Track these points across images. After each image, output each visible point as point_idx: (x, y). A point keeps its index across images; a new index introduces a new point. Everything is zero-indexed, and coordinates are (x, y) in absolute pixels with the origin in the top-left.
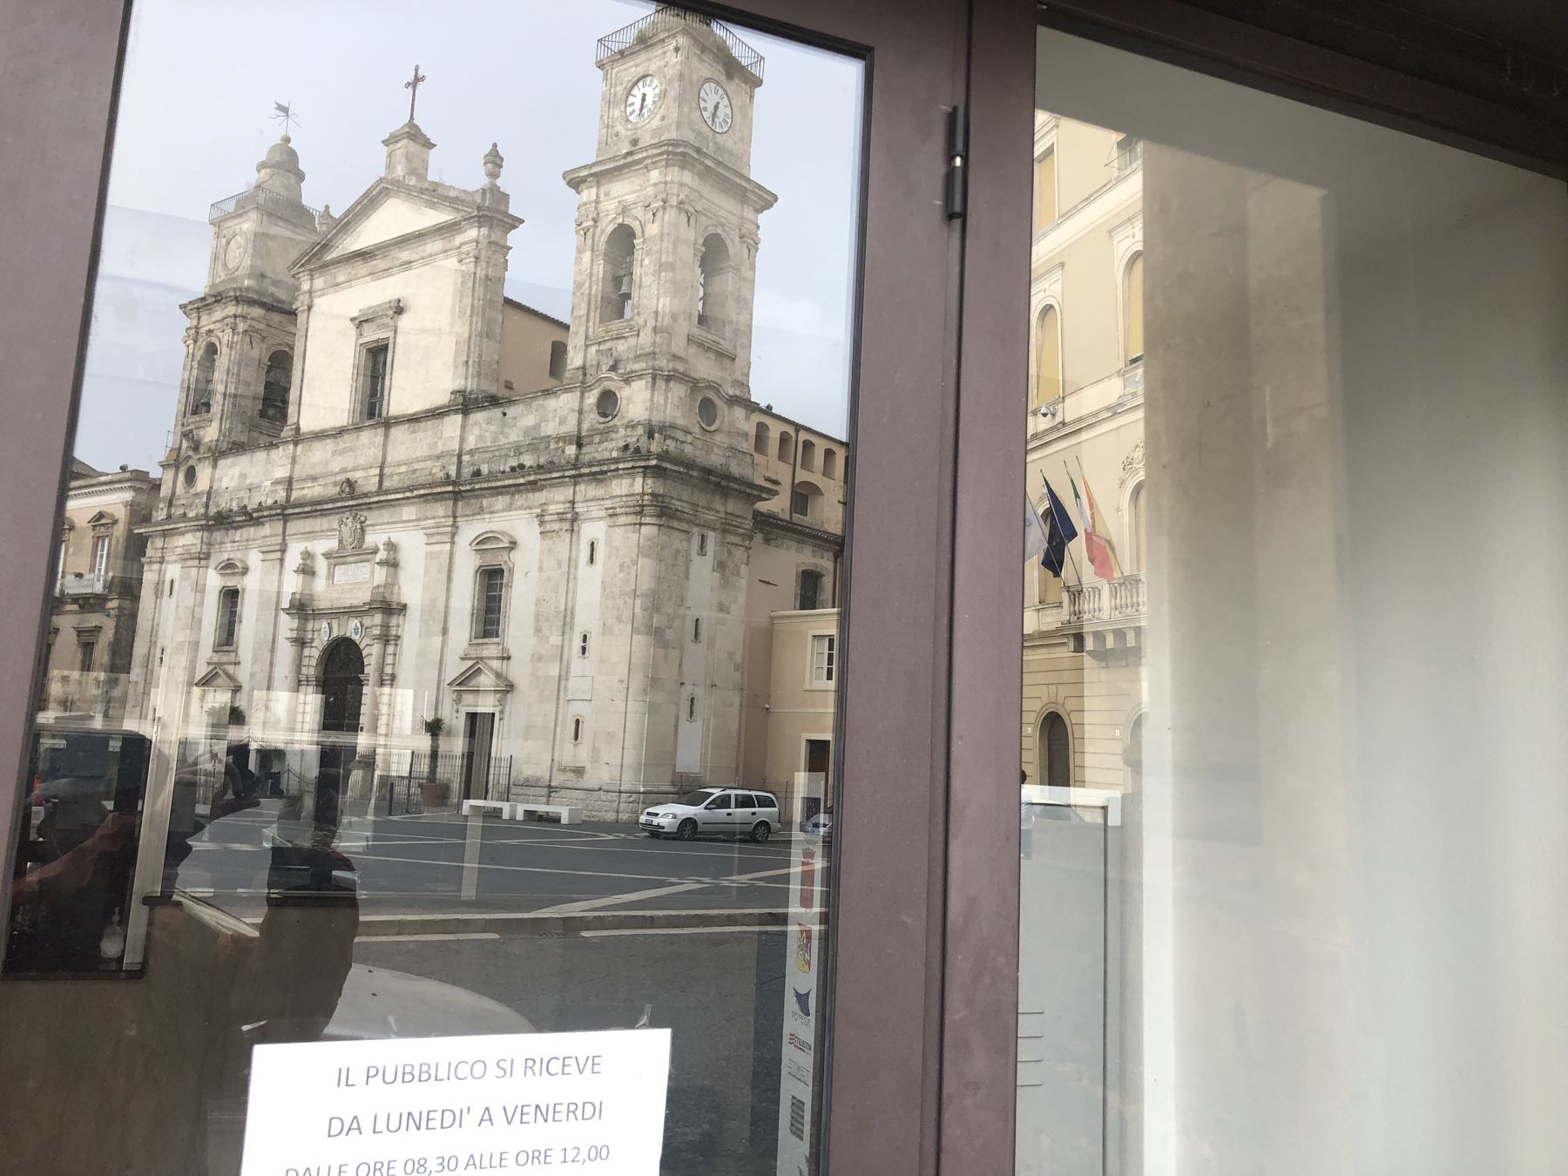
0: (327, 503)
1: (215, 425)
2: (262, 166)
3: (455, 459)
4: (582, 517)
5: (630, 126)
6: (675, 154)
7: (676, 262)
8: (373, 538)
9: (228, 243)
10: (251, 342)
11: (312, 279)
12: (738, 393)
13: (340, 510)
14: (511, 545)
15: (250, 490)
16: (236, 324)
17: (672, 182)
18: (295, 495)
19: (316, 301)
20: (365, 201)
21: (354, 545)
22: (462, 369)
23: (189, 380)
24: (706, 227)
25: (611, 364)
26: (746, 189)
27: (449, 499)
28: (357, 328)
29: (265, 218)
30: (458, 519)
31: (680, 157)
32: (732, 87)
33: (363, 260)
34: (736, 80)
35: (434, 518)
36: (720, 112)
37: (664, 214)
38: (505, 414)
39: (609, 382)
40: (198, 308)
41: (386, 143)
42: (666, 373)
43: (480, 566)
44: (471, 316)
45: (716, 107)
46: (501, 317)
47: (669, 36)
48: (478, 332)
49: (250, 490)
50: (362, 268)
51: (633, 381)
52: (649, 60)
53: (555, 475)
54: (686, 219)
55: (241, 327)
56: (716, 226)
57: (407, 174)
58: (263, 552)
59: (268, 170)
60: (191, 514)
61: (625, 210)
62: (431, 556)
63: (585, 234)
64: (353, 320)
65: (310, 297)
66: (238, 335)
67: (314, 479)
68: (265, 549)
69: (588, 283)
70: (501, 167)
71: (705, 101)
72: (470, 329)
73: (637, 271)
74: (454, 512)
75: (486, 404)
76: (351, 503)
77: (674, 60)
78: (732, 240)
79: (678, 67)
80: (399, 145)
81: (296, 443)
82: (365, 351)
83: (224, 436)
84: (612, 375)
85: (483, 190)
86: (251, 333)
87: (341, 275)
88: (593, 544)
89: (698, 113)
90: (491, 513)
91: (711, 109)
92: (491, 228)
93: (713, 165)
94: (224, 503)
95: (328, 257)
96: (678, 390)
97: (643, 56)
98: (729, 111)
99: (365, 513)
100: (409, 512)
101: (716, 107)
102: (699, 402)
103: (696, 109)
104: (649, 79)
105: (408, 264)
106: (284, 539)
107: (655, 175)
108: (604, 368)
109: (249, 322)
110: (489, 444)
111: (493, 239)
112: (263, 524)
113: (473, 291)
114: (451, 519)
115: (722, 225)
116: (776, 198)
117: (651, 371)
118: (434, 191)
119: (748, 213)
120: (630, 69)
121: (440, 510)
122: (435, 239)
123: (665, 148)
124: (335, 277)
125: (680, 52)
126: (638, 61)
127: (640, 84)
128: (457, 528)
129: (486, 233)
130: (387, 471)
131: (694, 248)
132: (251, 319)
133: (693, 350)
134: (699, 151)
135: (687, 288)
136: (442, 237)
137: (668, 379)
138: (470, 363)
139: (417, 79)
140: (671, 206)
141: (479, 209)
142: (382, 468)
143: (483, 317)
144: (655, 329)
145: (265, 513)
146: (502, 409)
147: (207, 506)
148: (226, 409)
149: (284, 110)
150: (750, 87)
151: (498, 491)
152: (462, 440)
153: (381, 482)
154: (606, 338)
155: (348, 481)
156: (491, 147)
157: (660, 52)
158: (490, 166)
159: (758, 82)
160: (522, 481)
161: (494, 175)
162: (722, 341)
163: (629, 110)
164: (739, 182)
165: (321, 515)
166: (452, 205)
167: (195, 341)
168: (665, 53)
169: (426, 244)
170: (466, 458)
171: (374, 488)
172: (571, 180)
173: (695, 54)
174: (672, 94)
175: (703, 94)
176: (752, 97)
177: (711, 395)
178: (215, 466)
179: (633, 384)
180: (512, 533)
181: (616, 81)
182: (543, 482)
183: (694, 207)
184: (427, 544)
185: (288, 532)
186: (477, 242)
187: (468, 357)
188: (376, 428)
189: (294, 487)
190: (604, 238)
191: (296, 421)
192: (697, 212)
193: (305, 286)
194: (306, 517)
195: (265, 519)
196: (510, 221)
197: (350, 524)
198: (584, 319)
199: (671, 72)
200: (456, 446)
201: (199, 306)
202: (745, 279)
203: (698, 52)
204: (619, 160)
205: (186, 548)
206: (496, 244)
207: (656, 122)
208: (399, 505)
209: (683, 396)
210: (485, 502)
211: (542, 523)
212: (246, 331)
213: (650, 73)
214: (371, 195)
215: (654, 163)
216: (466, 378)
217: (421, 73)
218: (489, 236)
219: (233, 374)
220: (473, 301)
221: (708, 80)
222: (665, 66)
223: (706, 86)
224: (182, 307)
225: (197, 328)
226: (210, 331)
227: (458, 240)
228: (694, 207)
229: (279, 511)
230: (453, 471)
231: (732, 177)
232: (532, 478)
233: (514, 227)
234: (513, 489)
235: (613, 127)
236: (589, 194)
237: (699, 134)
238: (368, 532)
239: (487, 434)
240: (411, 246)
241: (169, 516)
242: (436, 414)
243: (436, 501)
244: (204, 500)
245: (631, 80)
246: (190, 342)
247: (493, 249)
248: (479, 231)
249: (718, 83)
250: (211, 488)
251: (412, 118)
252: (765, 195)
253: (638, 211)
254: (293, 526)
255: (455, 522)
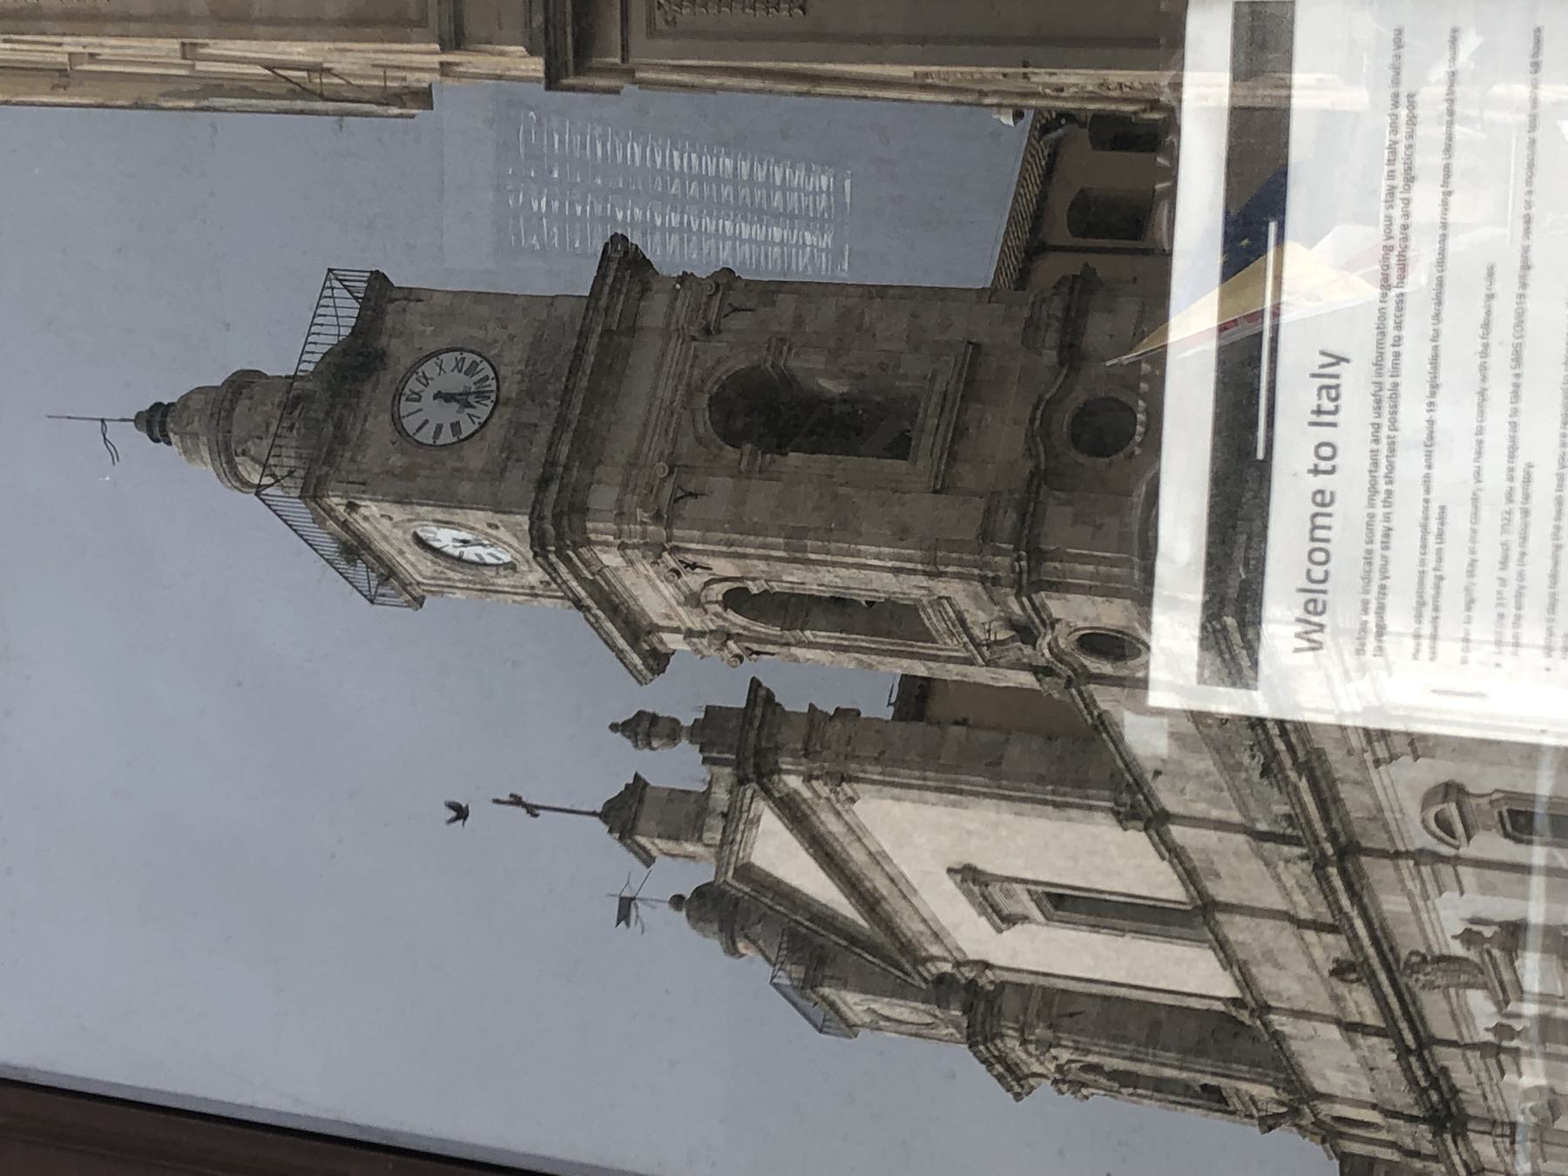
0: (1387, 1004)
1: (1244, 1086)
2: (732, 951)
3: (1268, 846)
4: (1375, 702)
5: (524, 568)
6: (560, 536)
7: (782, 527)
8: (1457, 949)
9: (888, 1019)
10: (1071, 1015)
11: (933, 959)
12: (1052, 338)
13: (1407, 997)
14: (1453, 796)
15: (1372, 1069)
16: (1037, 1042)
17: (618, 535)
18: (1372, 1018)
19: (972, 956)
20: (766, 900)
21: (1476, 972)
22: (1073, 813)
23: (1160, 1100)
24: (699, 440)
25: (1019, 644)
26: (607, 332)
27: (1360, 871)
28: (1014, 924)
29: (828, 972)
30: (1402, 849)
31: (565, 523)
32: (400, 353)
33: (878, 902)
34: (383, 341)
35: (1402, 881)
36: (457, 382)
37: (688, 550)
38: (1157, 773)
39: (1062, 642)
40: (1018, 1080)
41: (648, 860)
42: (1024, 563)
43: (1507, 835)
44: (961, 792)
45: (447, 397)
46: (956, 730)
47: (336, 520)
48: (991, 783)
49: (1372, 1069)
50: (893, 903)
51: (1050, 616)
52: (385, 538)
53: (1280, 745)
54: (691, 501)
55: (1040, 1031)
56: (693, 411)
57: (700, 839)
58: (1503, 1073)
59: (741, 946)
60: (1430, 1137)
61: (694, 600)
62: (1486, 889)
63: (758, 653)
64: (1000, 931)
65: (968, 963)
66: (1060, 1038)
67: (1336, 999)
68: (1495, 1074)
69: (857, 655)
70: (654, 719)
71: (439, 428)
72: (985, 795)
73: (813, 589)
74: (1383, 854)
75: (1141, 797)
76: (1383, 977)
77: (371, 508)
78: (719, 362)
79: (386, 505)
80: (649, 846)
81: (1268, 1009)
82: (1060, 913)
83: (1267, 1075)
84: (1043, 643)
85: (705, 761)
86: (1054, 1012)
87: (911, 926)
88: (1434, 691)
89: (468, 450)
90: (1380, 809)
91: (450, 412)
92: (777, 749)
93: (567, 437)
94: (1403, 1099)
95: (880, 937)
96: (1058, 526)
97: (382, 546)
98: (449, 359)
99: (1404, 954)
100: (1392, 904)
101: (447, 397)
102: (1082, 458)
103: (461, 458)
104: (421, 534)
105: (877, 858)
106: (1474, 1046)
107: (611, 559)
108: (1028, 650)
109: (1031, 1017)
110: (1226, 794)
111: (799, 746)
112: (1444, 1071)
113: (910, 787)
114: (1402, 862)
115: (691, 392)
116: (618, 240)
117: (1025, 600)
118: (725, 815)
119: (655, 310)
120: (415, 565)
121: (1377, 871)
122: (818, 824)
123: (553, 558)
124: (922, 933)
125: (358, 502)
126: (393, 552)
127: (437, 545)
128: (1421, 851)
129: (789, 759)
130: (1305, 915)
131: (748, 475)
132: (1025, 1010)
133: (967, 476)
134: (543, 483)
135: (835, 496)
136: (809, 812)
137: (1037, 555)
138: (1059, 799)
139: (516, 801)
140: (669, 540)
141: (742, 781)
142: (1300, 924)
143: (956, 769)
144: (940, 574)
145: (1419, 1073)
146: (1149, 776)
147: (1412, 1119)
148: (1209, 1069)
149: (625, 908)
150: (392, 301)
151: (1328, 801)
152: (1220, 825)
153: (1333, 929)
154: (966, 639)
155: (1333, 973)
156: (619, 734)
157: (366, 525)
158: (655, 744)
159: (378, 279)
160: (1303, 784)
161: (672, 731)
162: (939, 387)
163: (490, 560)
164: (592, 358)
165: (1414, 1003)
166: (745, 808)
167: (1084, 1085)
168: (366, 518)
169: (830, 832)
170: (1262, 826)
171: (1342, 939)
172: (651, 670)
173: (352, 460)
174: (440, 514)
175: (426, 436)
176: (411, 295)
177: (1063, 420)
178: (1329, 1098)
179: (1056, 615)
180: (1425, 789)
181: (440, 579)
182: (1301, 755)
183: (663, 480)
184: (1462, 893)
185: (1454, 1036)
186: (809, 778)
187: (1045, 802)
188: (1217, 923)
189: (1357, 1019)
190: (760, 628)
191: (1219, 1003)
192: (671, 473)
193: (947, 968)
194: (1422, 1019)
195: (1433, 1069)
196: (758, 712)
197: (1428, 977)
198: (931, 664)
199: (398, 513)
200: (1241, 839)
201: (1014, 1078)
202: (799, 322)
203: (348, 455)
204: (595, 616)
205: (1503, 1153)
206: (807, 741)
207: (503, 533)
208: (1383, 921)
209: (1069, 509)
210: (1356, 814)
211: (1392, 758)
212: (1050, 1026)
213: (409, 537)
214: (753, 893)
215: (587, 564)
216: (1090, 808)
217: (506, 798)
218: (794, 754)
219: (1139, 1052)
220: (928, 788)
221: (396, 420)
222: (390, 519)
223: (410, 424)
224: (1018, 1097)
225: (1055, 1082)
226: (1059, 1068)
227: (807, 794)
228: (663, 480)
229: (1413, 1059)
230: (1297, 851)
231: (584, 383)
232: (1293, 775)
233: (770, 696)
234: (1323, 785)
235: (532, 588)
236: (674, 642)
237: (508, 447)
238: (1445, 952)
239: (1203, 794)
240: (839, 848)
241: (1435, 1158)
242: (1173, 853)
243: (1361, 874)
244: (1401, 1122)
245: (434, 563)
246: (1085, 1091)
247: (818, 748)
248: (788, 772)
249: (398, 395)
250: (1374, 1107)
251: (594, 814)
252: (610, 280)
253: (694, 580)
254: (1440, 1025)
255: (1408, 854)
